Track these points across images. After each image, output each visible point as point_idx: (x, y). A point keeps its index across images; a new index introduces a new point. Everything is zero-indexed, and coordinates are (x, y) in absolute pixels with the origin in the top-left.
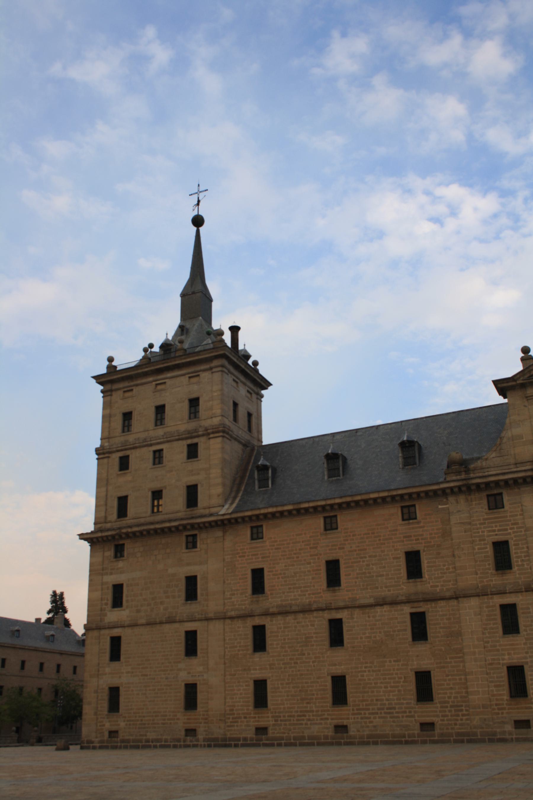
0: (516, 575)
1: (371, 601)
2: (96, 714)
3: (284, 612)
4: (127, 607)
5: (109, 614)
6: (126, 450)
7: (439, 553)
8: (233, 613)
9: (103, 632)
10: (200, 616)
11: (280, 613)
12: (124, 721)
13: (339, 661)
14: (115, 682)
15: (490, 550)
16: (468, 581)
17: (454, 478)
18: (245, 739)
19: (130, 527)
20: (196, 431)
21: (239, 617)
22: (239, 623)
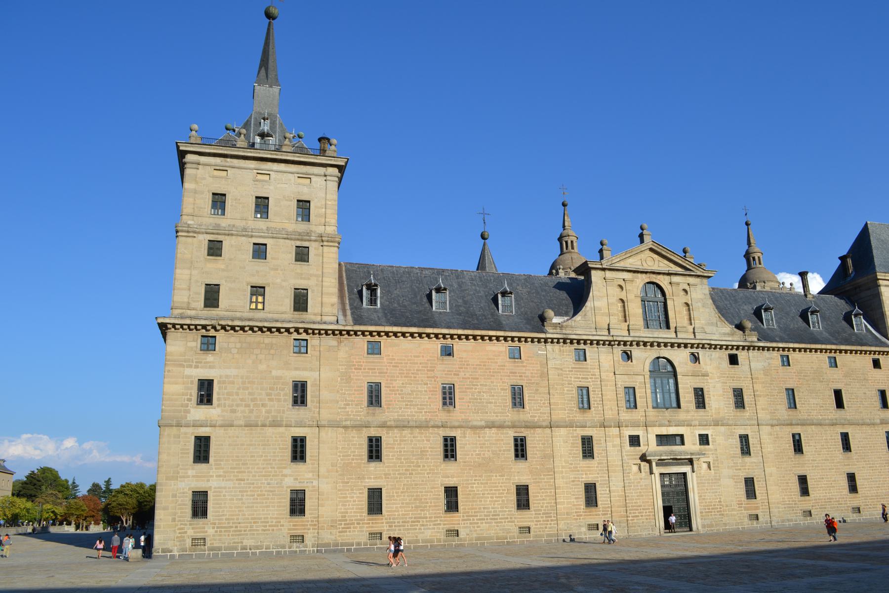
0: (594, 415)
1: (483, 423)
2: (174, 520)
3: (402, 426)
4: (218, 406)
5: (192, 410)
6: (217, 234)
7: (537, 390)
8: (348, 423)
9: (183, 430)
10: (311, 423)
11: (396, 427)
12: (213, 528)
13: (451, 473)
14: (201, 486)
15: (575, 392)
16: (560, 415)
17: (551, 331)
18: (359, 544)
19: (240, 319)
20: (308, 234)
21: (354, 427)
22: (353, 433)
